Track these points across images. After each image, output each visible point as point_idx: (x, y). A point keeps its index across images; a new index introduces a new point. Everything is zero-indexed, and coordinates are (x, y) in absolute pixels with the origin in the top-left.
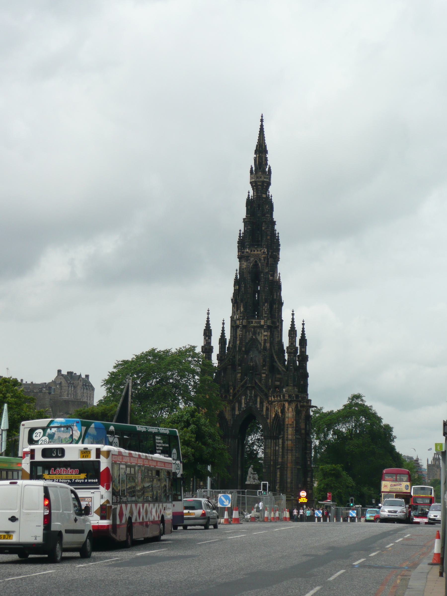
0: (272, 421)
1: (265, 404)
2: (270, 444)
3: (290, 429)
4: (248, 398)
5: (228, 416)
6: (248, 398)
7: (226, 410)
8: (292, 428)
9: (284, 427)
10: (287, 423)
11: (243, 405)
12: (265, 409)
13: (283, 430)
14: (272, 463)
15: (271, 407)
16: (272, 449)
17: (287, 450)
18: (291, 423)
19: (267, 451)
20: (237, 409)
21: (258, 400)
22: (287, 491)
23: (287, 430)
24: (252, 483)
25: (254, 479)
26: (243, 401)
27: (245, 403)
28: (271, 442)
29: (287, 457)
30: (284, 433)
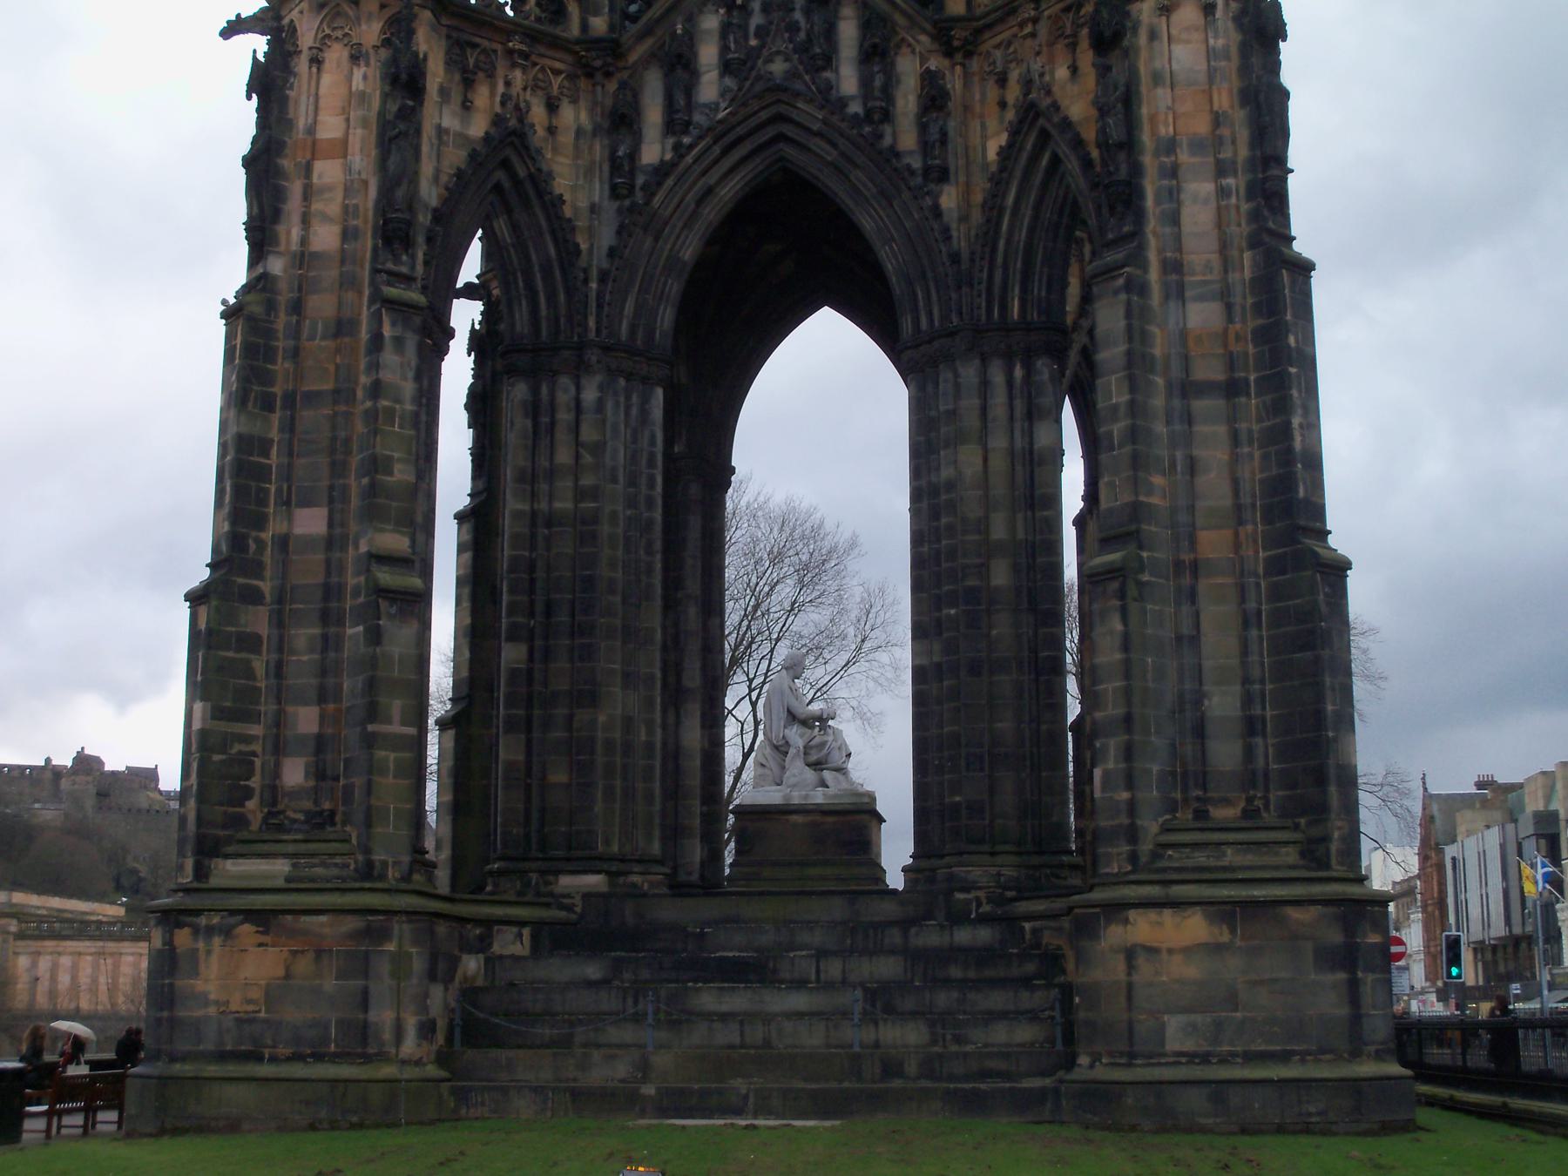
0: (978, 198)
1: (908, 68)
2: (970, 403)
3: (1199, 190)
4: (756, 20)
5: (574, 179)
6: (756, 20)
7: (552, 130)
8: (1221, 170)
9: (1136, 170)
10: (1165, 131)
11: (709, 87)
12: (907, 101)
13: (1123, 197)
14: (1001, 575)
15: (967, 76)
16: (998, 442)
17: (1187, 389)
18: (1202, 126)
19: (946, 473)
20: (653, 115)
21: (848, 31)
22: (1201, 814)
23: (1173, 195)
24: (796, 798)
25: (817, 766)
26: (708, 54)
27: (727, 67)
28: (985, 384)
29: (1192, 467)
30: (1140, 216)
